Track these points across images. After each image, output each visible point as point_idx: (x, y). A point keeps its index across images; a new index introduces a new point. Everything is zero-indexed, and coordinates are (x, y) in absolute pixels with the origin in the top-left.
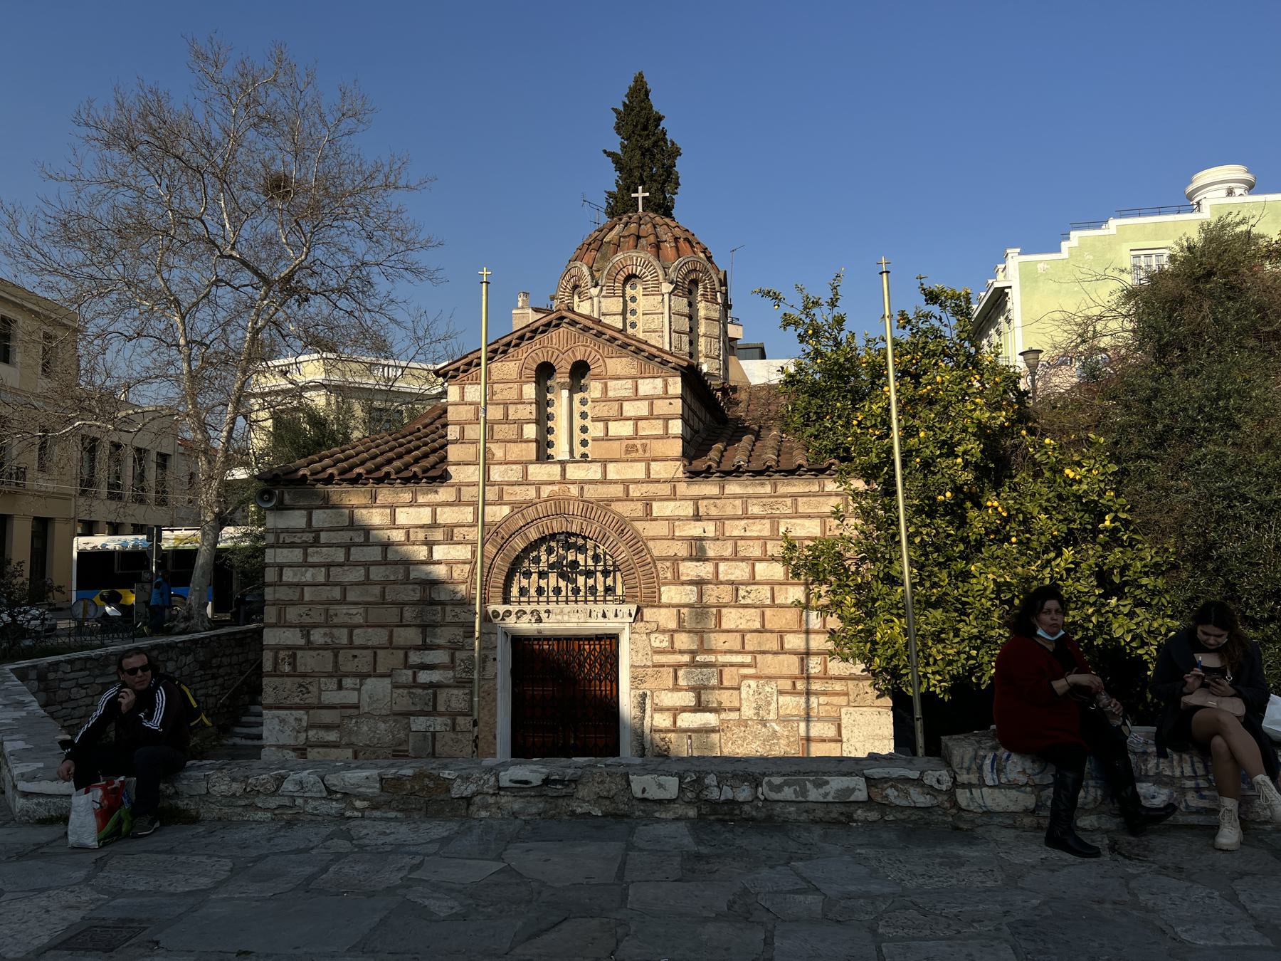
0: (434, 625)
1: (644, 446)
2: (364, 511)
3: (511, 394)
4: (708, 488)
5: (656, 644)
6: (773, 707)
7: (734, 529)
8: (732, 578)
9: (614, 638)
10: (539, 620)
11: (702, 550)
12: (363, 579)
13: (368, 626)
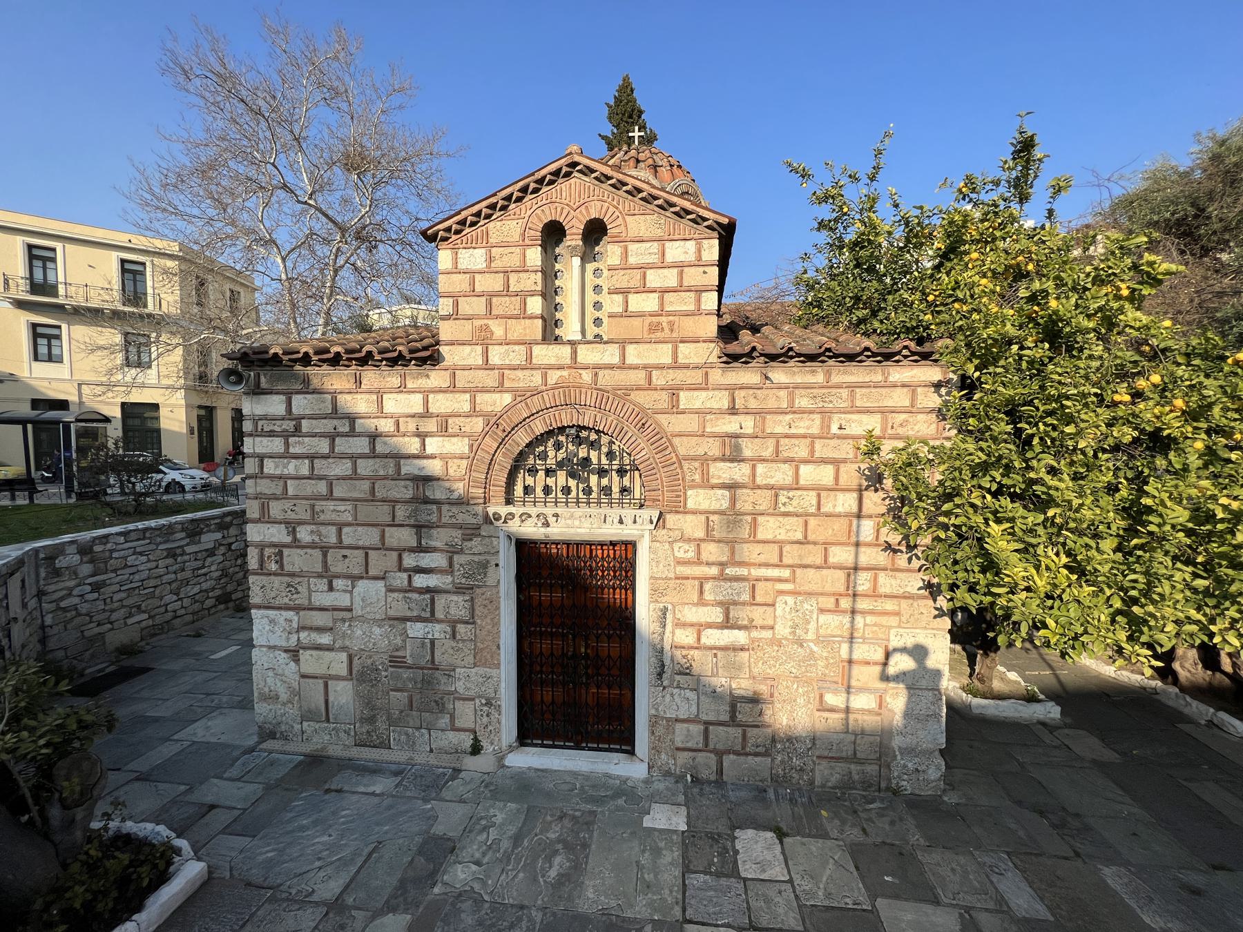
0: (430, 526)
1: (671, 324)
2: (348, 397)
3: (515, 261)
4: (747, 375)
5: (680, 555)
6: (812, 626)
7: (778, 425)
8: (772, 482)
9: (630, 546)
10: (547, 524)
11: (738, 448)
12: (349, 472)
13: (357, 525)
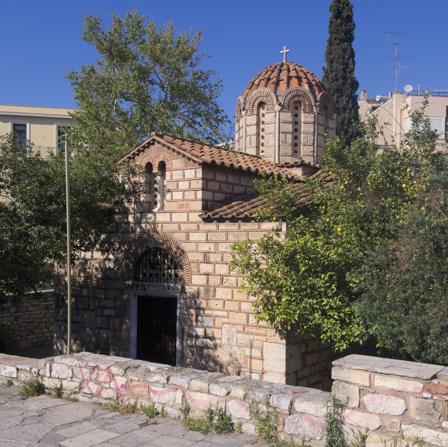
4: (212, 226)
10: (145, 289)
